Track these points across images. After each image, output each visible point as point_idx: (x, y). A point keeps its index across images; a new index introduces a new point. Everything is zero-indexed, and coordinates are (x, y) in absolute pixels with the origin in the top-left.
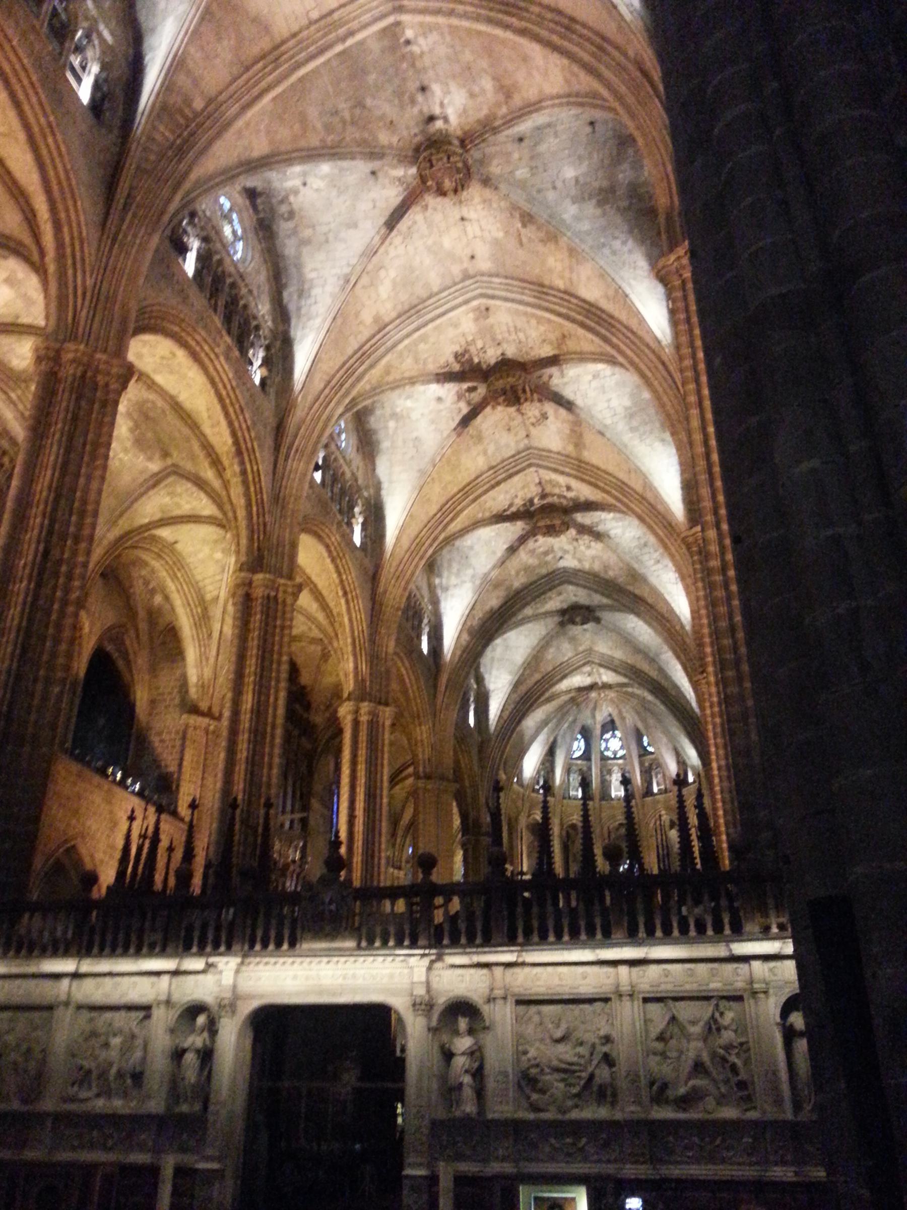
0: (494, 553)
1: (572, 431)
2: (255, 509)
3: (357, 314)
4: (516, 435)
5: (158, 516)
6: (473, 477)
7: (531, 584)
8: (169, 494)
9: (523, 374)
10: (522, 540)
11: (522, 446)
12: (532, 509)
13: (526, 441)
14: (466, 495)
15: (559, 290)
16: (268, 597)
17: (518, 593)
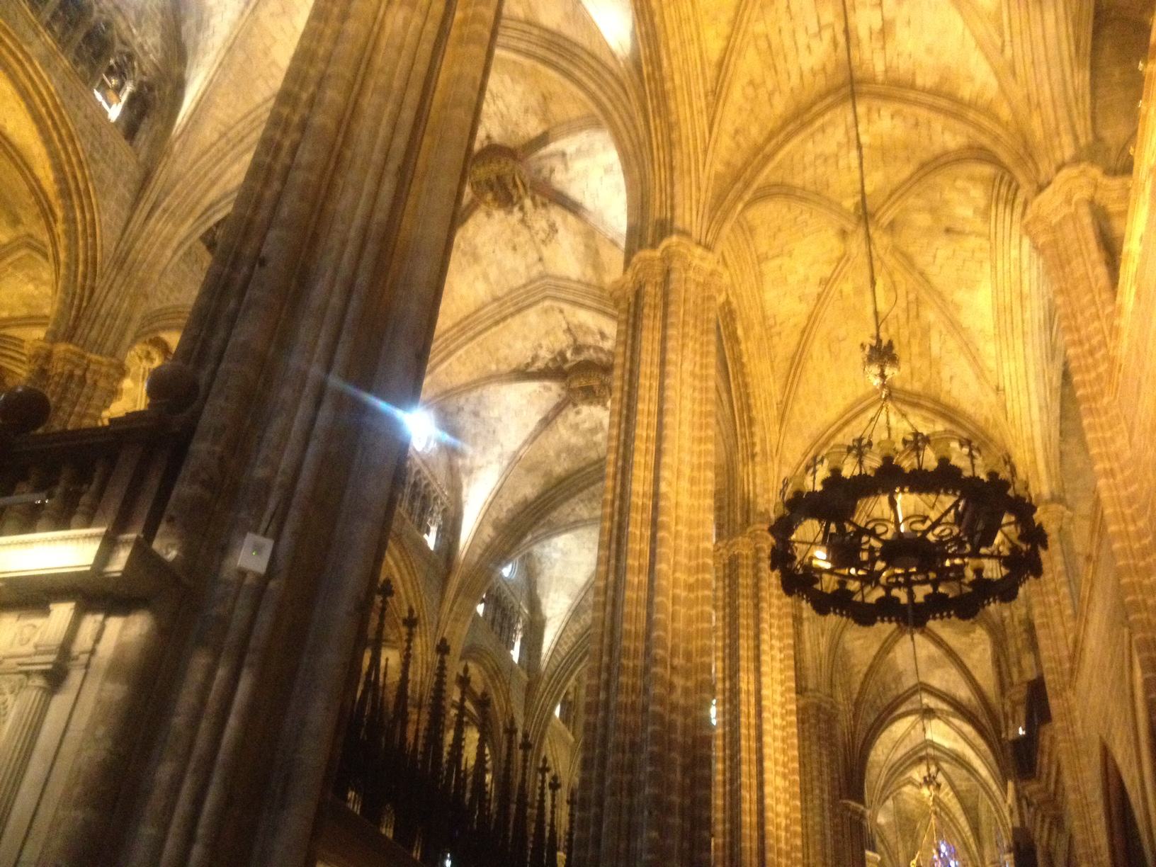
0: (526, 426)
1: (587, 246)
2: (81, 268)
3: (266, 52)
4: (525, 255)
5: (23, 312)
6: (473, 309)
7: (579, 471)
8: (32, 279)
9: (511, 162)
10: (559, 409)
11: (534, 272)
12: (566, 366)
13: (540, 267)
14: (463, 331)
15: (519, 21)
16: (71, 376)
17: (561, 481)
